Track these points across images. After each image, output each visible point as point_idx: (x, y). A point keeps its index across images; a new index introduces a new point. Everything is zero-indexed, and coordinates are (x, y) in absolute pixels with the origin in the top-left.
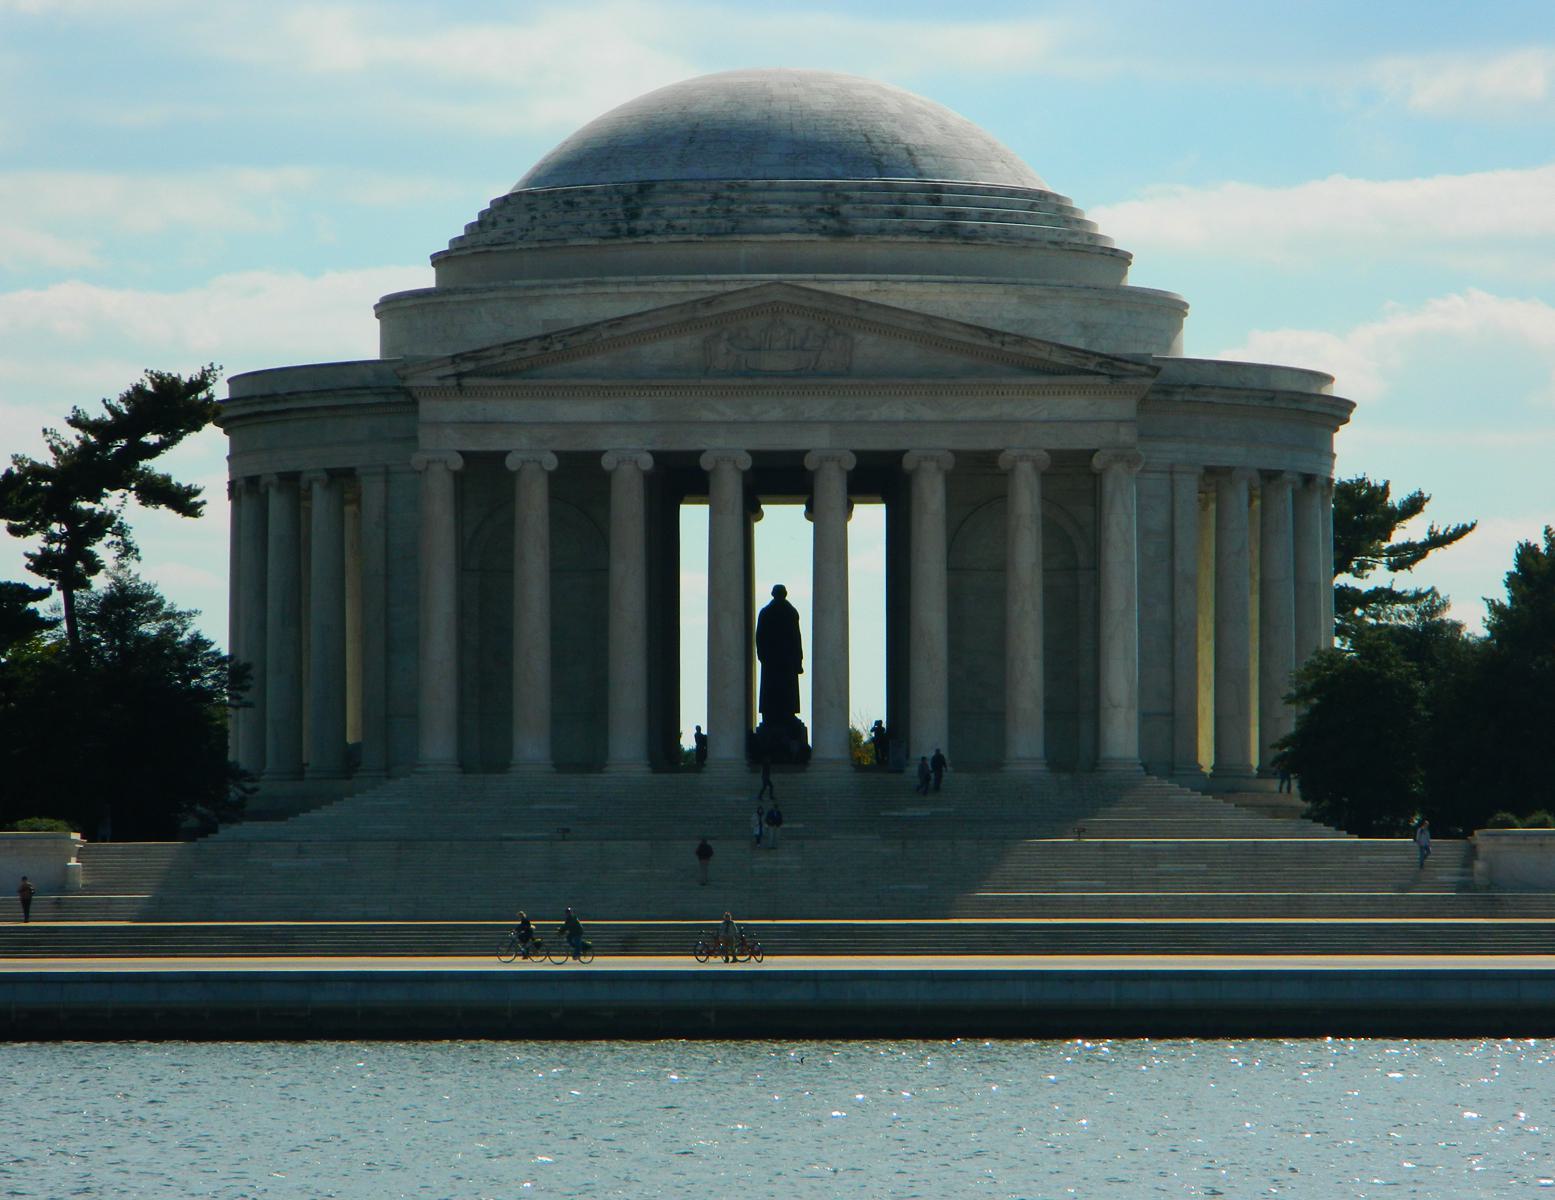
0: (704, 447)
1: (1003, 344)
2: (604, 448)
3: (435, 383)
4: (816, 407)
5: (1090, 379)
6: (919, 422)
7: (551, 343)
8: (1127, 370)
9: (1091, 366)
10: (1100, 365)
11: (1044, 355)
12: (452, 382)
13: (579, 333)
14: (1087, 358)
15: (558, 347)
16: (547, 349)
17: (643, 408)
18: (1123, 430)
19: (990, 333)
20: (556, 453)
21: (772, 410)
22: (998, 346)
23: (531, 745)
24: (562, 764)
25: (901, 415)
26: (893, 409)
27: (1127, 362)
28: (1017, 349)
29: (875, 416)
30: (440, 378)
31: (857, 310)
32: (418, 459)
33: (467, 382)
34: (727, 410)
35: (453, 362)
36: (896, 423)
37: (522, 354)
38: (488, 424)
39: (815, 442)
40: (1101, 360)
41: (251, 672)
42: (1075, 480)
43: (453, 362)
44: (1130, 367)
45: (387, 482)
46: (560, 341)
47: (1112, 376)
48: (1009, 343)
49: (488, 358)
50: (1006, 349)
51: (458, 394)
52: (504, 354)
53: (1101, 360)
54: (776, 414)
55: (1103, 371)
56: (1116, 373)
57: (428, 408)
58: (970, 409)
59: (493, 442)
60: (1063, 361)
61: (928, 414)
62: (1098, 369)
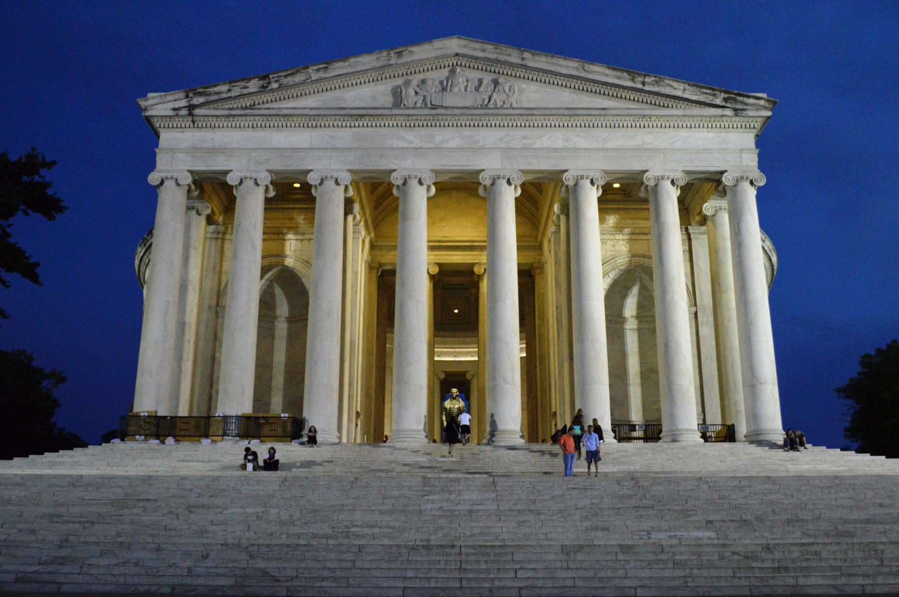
0: (393, 167)
1: (644, 84)
3: (171, 113)
4: (489, 137)
5: (719, 111)
6: (576, 149)
7: (269, 83)
8: (746, 104)
9: (718, 102)
10: (725, 100)
12: (184, 112)
13: (290, 74)
14: (714, 95)
15: (275, 86)
16: (266, 87)
17: (344, 136)
22: (640, 86)
25: (560, 144)
28: (655, 89)
29: (538, 145)
30: (174, 109)
31: (523, 59)
32: (153, 178)
33: (197, 112)
34: (413, 138)
35: (187, 97)
36: (555, 150)
37: (245, 91)
38: (214, 151)
39: (489, 164)
40: (726, 96)
43: (187, 97)
46: (276, 81)
47: (735, 110)
48: (649, 84)
49: (216, 93)
50: (647, 88)
51: (192, 125)
52: (229, 91)
53: (726, 96)
54: (455, 143)
55: (728, 105)
56: (739, 106)
57: (166, 137)
58: (618, 139)
59: (217, 164)
60: (694, 98)
62: (724, 104)
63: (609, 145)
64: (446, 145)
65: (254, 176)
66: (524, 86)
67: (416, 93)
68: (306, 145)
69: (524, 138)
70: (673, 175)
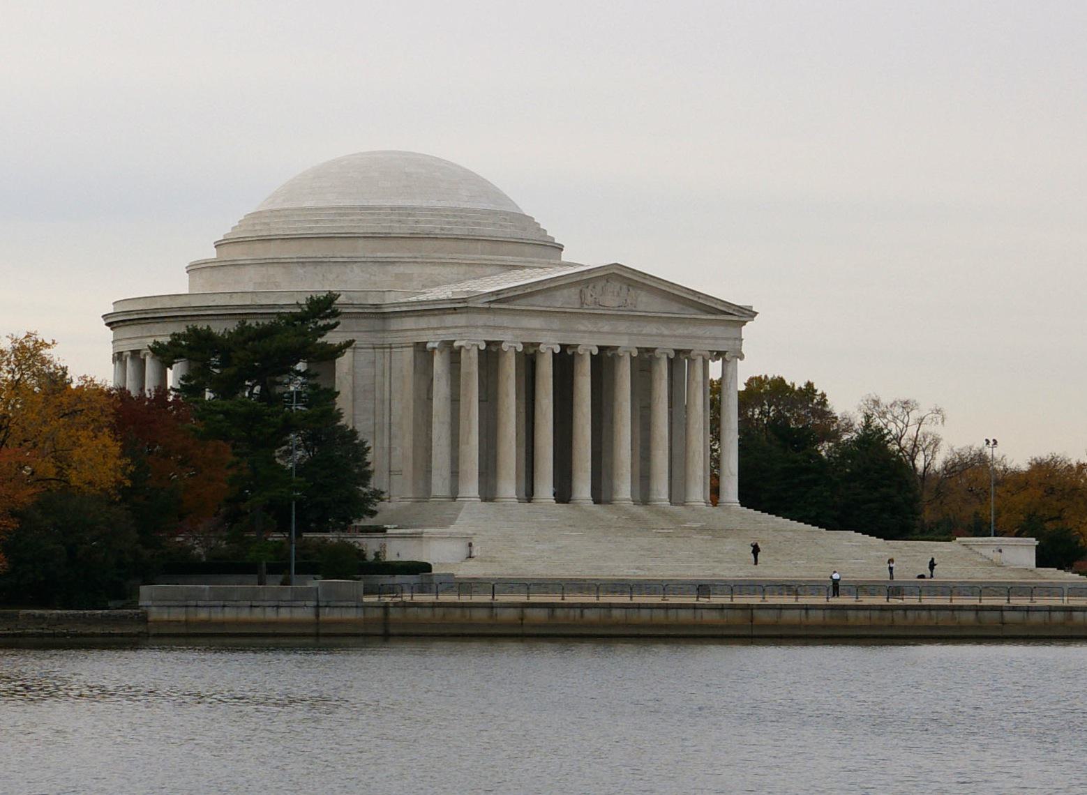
1: (699, 298)
2: (540, 341)
4: (622, 326)
7: (527, 288)
8: (744, 313)
9: (731, 312)
11: (713, 305)
17: (556, 323)
18: (737, 342)
20: (523, 343)
21: (606, 327)
22: (696, 299)
23: (508, 486)
24: (597, 498)
25: (655, 331)
26: (651, 328)
27: (746, 309)
29: (644, 332)
38: (495, 327)
41: (370, 451)
45: (354, 352)
48: (702, 298)
56: (741, 315)
58: (681, 331)
61: (666, 332)
62: (734, 313)
65: (514, 345)
66: (639, 292)
67: (591, 296)
68: (538, 326)
69: (639, 326)
70: (704, 353)
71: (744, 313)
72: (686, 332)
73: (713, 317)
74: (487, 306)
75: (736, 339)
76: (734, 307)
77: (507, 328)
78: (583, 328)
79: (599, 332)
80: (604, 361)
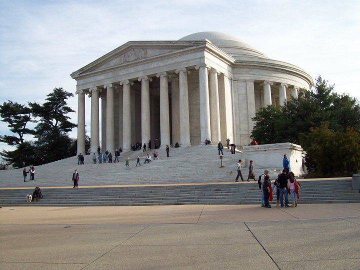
4: (140, 68)
9: (192, 45)
11: (182, 45)
17: (110, 75)
19: (170, 42)
21: (132, 70)
33: (81, 75)
34: (124, 72)
42: (193, 75)
44: (200, 42)
61: (161, 65)
63: (167, 63)
64: (131, 72)
71: (198, 44)
72: (172, 62)
73: (182, 50)
74: (79, 76)
75: (200, 58)
76: (193, 42)
77: (91, 82)
78: (121, 74)
79: (130, 73)
80: (136, 86)
